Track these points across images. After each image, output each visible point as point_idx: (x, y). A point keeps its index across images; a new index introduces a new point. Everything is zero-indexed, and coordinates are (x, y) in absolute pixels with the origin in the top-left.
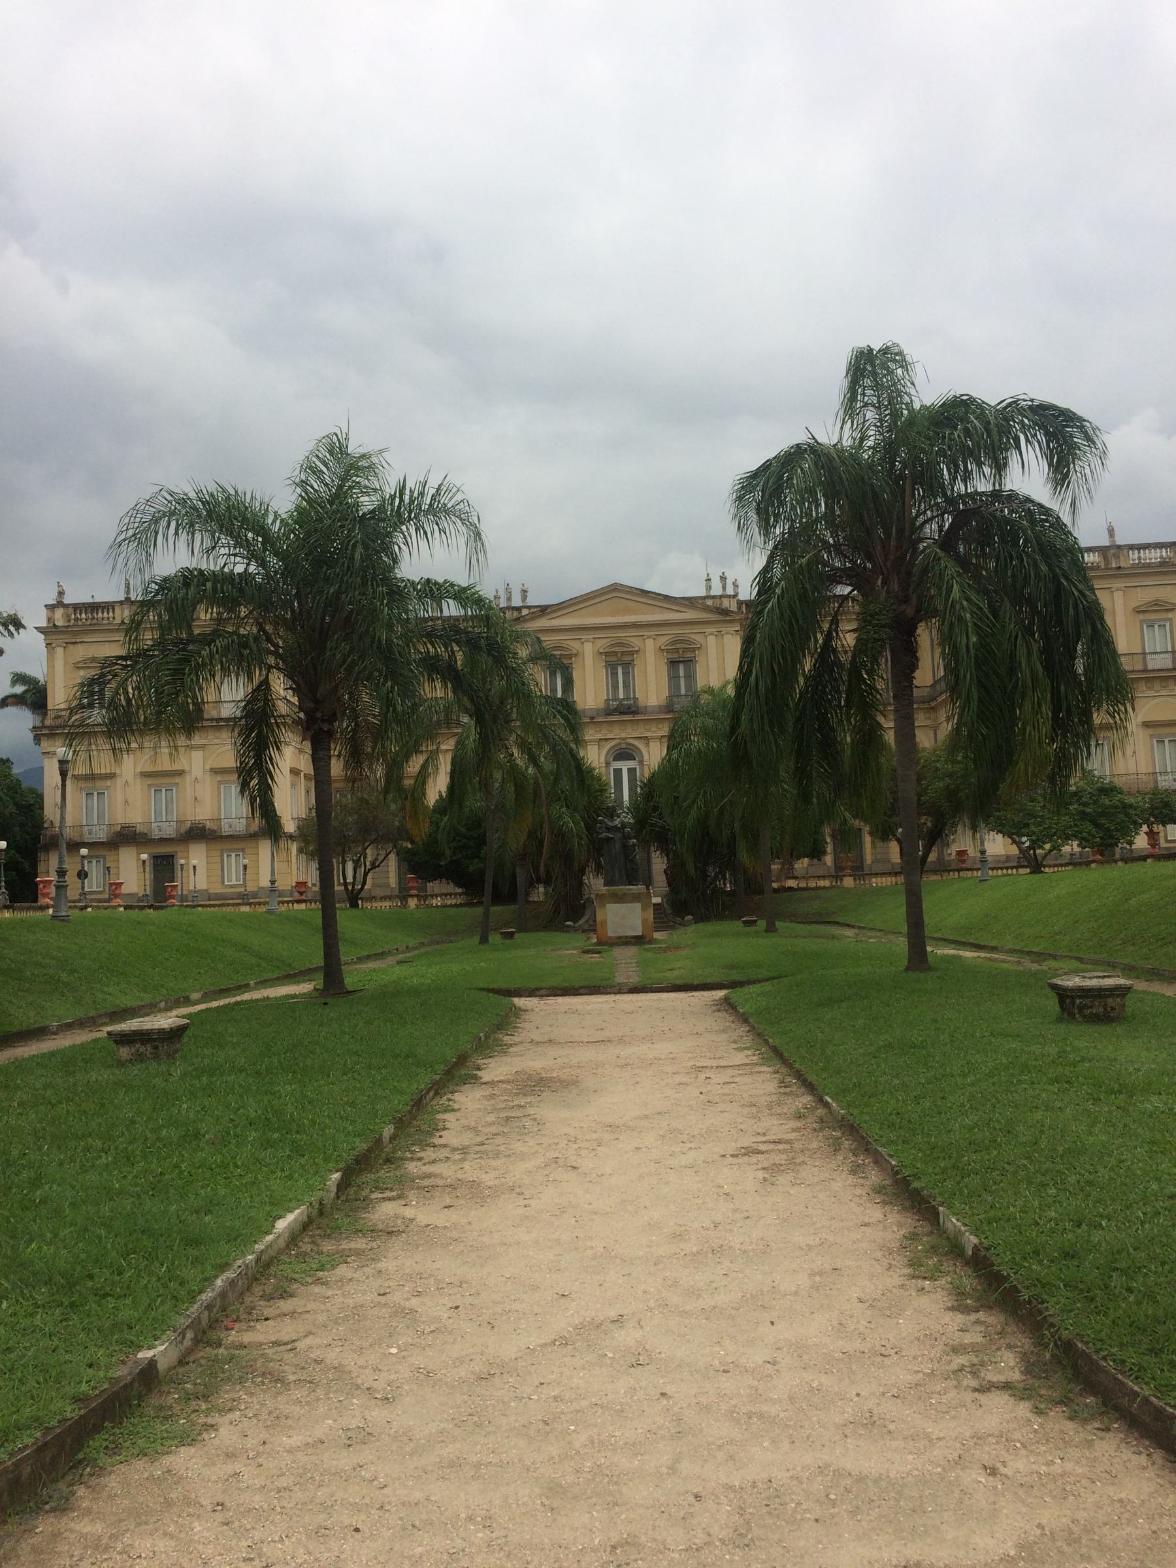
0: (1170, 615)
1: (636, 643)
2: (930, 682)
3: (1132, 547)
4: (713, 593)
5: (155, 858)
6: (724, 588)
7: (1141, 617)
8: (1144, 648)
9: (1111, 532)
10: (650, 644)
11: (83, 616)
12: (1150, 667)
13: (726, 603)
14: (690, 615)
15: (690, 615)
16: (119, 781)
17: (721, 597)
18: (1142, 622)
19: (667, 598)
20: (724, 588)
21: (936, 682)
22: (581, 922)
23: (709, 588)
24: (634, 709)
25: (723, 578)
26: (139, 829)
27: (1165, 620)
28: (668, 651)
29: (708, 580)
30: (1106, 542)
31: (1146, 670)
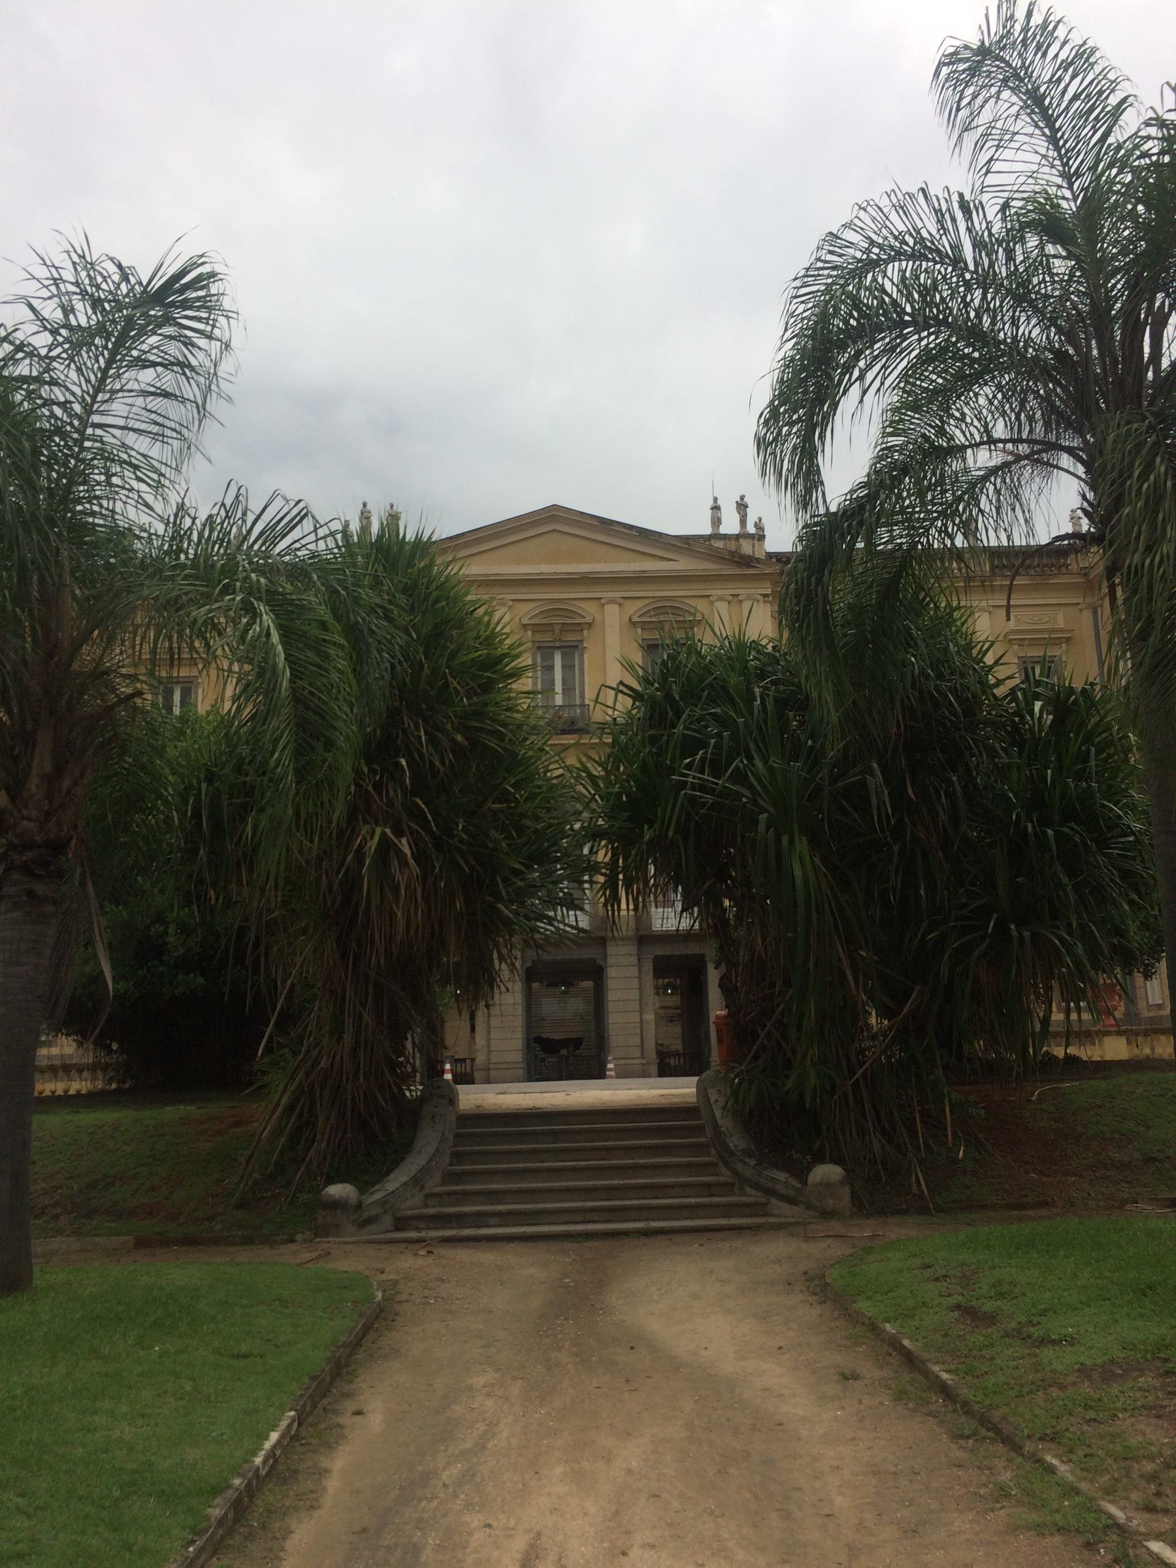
1: (589, 610)
4: (724, 529)
6: (743, 522)
10: (612, 611)
13: (746, 548)
14: (683, 564)
15: (683, 564)
17: (737, 537)
19: (644, 534)
20: (743, 522)
22: (396, 1181)
23: (716, 521)
24: (581, 724)
25: (742, 506)
28: (645, 626)
29: (716, 508)
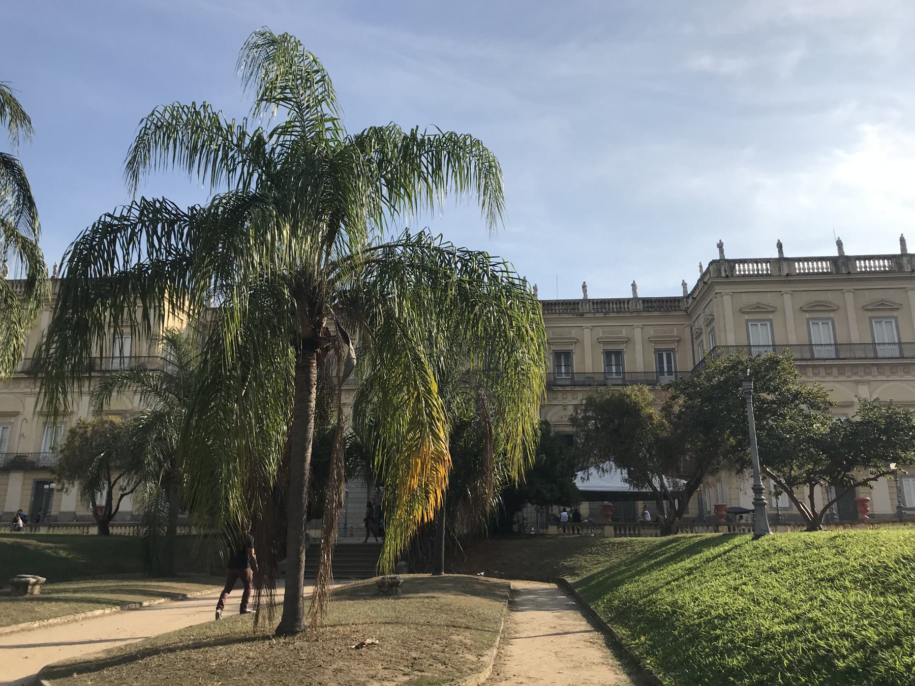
0: (895, 314)
2: (690, 367)
3: (859, 258)
5: (39, 484)
7: (870, 314)
8: (873, 338)
9: (839, 244)
11: (18, 290)
12: (880, 355)
16: (21, 418)
18: (871, 318)
21: (695, 367)
26: (31, 458)
27: (892, 317)
30: (835, 253)
31: (876, 358)
